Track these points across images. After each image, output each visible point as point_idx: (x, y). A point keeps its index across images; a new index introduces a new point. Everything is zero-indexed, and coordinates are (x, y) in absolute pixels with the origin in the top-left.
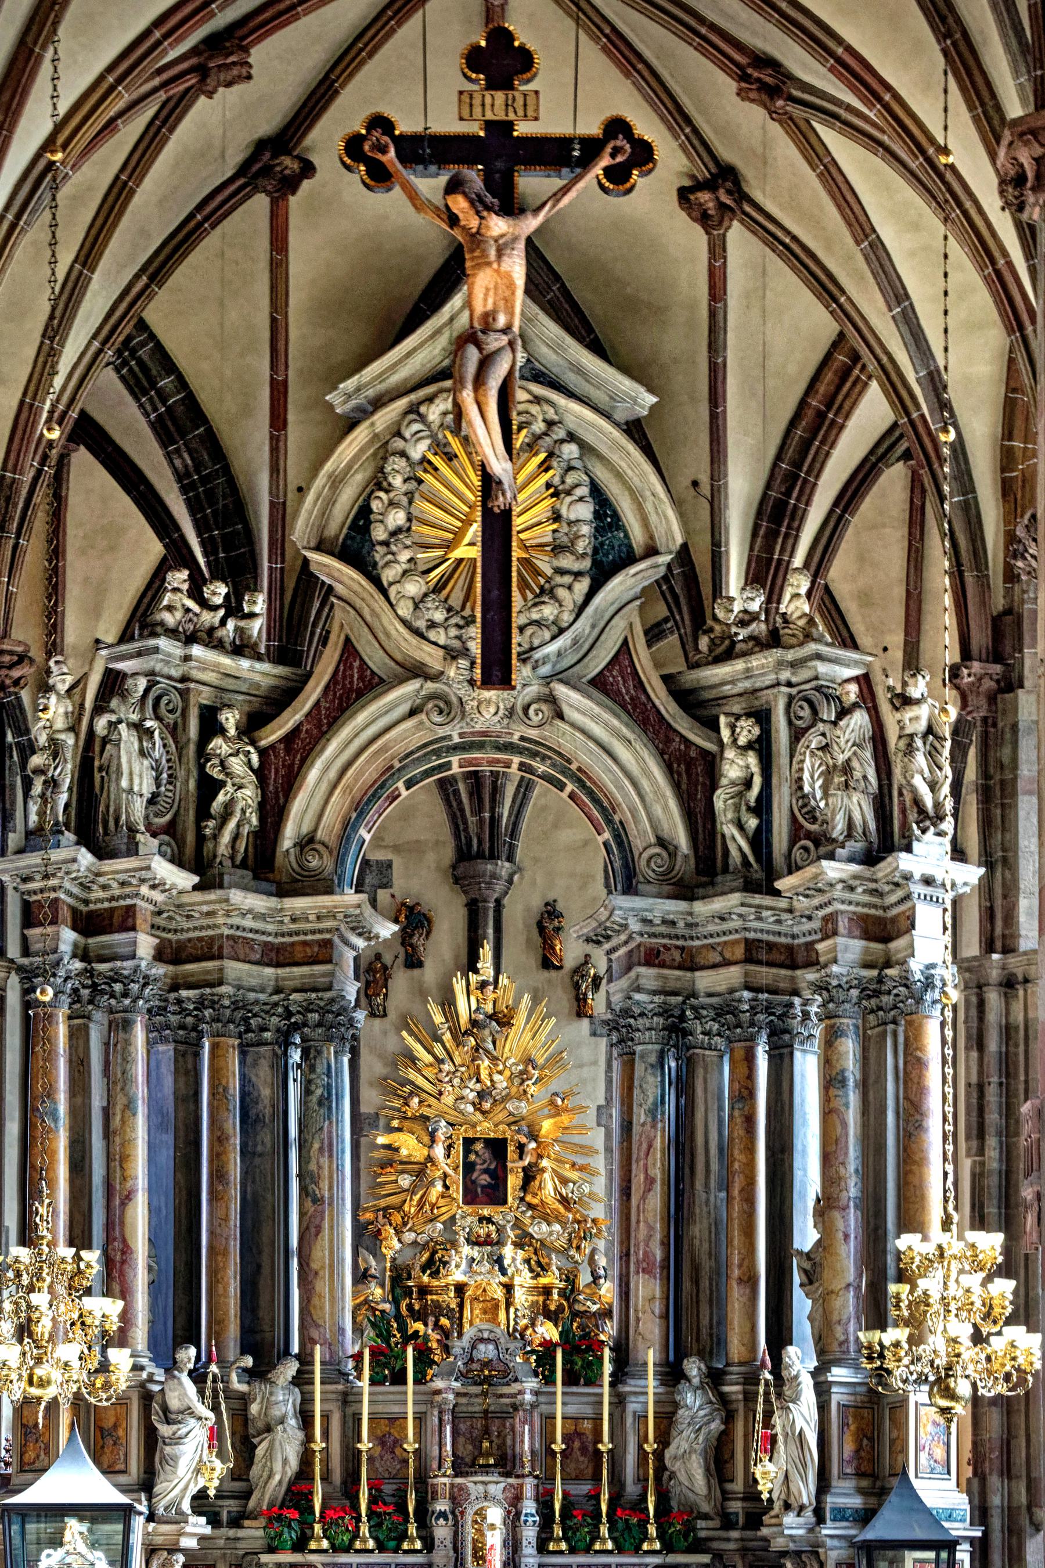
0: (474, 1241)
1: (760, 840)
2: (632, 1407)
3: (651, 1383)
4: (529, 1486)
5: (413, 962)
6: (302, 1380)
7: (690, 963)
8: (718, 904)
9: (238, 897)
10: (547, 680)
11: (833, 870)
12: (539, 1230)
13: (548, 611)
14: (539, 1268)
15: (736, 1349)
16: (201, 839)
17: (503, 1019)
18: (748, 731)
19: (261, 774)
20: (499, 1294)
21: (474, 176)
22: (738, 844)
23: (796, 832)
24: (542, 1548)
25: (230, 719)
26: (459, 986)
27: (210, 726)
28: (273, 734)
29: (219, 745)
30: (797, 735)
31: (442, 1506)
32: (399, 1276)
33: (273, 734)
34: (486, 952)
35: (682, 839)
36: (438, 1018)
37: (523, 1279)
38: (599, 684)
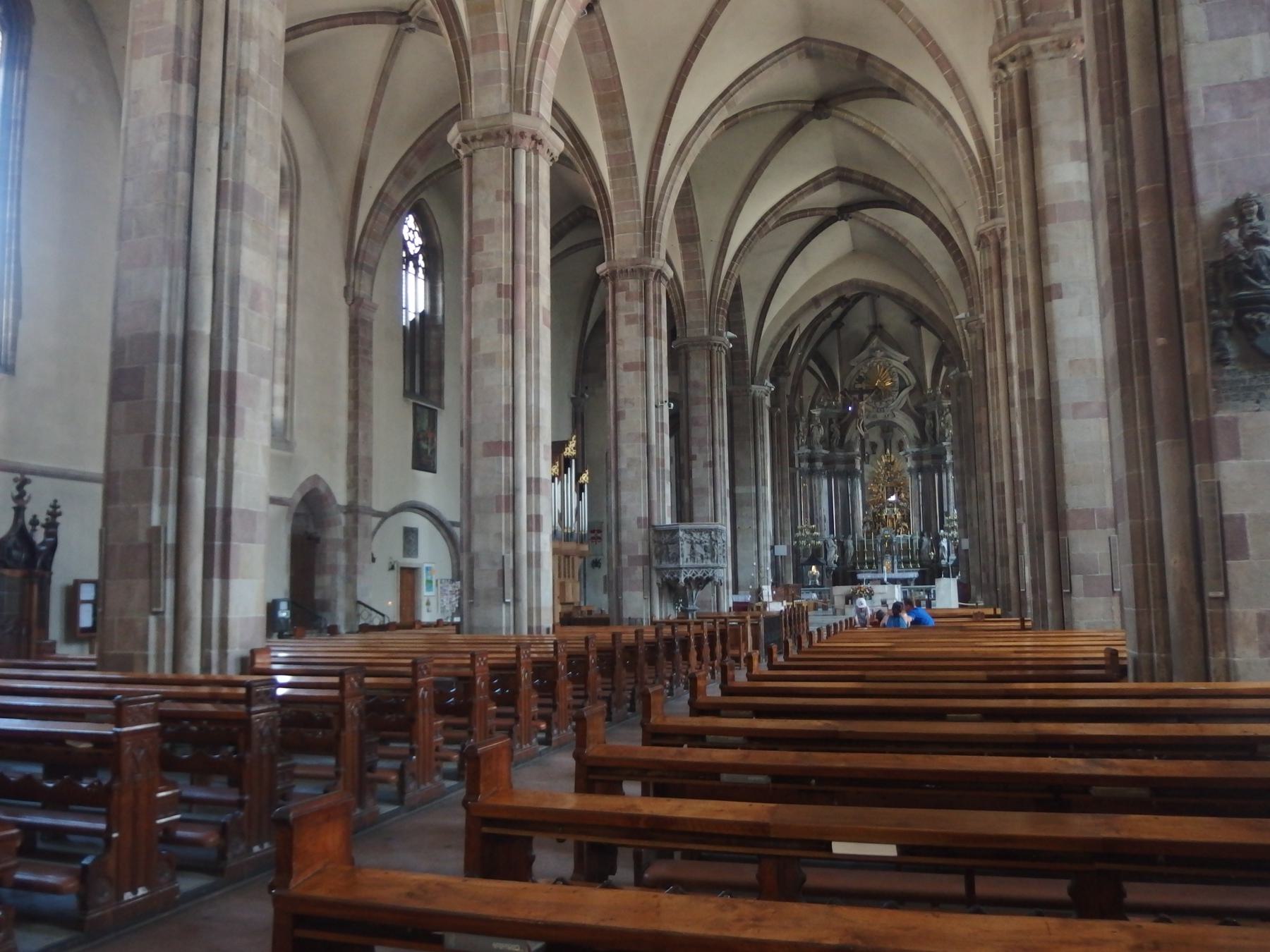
0: (888, 507)
1: (934, 436)
2: (914, 541)
3: (918, 537)
4: (895, 557)
5: (874, 453)
6: (853, 539)
7: (922, 459)
8: (926, 449)
9: (837, 454)
10: (892, 410)
11: (944, 444)
12: (902, 504)
13: (891, 398)
14: (902, 512)
15: (933, 527)
16: (830, 443)
17: (892, 463)
18: (930, 416)
19: (840, 429)
20: (893, 516)
21: (857, 396)
22: (929, 437)
23: (941, 433)
24: (899, 567)
25: (834, 421)
26: (883, 457)
27: (831, 422)
28: (843, 421)
29: (832, 426)
30: (940, 415)
31: (880, 561)
32: (874, 514)
33: (843, 421)
34: (888, 451)
35: (918, 436)
36: (879, 464)
37: (899, 515)
38: (902, 409)
